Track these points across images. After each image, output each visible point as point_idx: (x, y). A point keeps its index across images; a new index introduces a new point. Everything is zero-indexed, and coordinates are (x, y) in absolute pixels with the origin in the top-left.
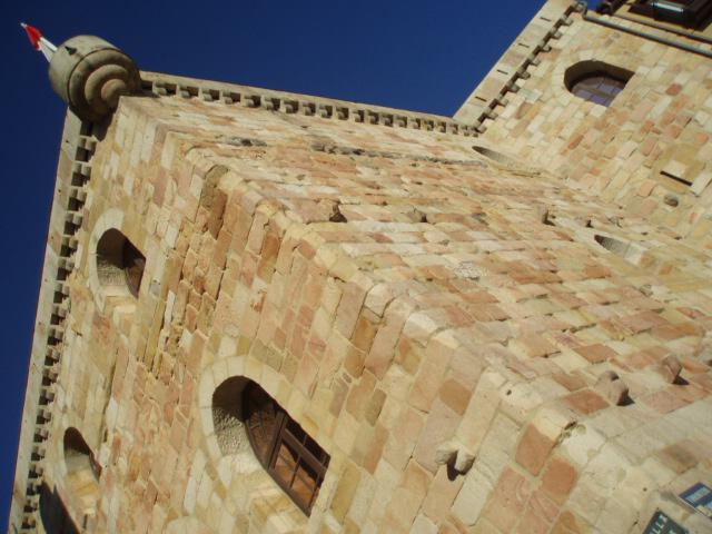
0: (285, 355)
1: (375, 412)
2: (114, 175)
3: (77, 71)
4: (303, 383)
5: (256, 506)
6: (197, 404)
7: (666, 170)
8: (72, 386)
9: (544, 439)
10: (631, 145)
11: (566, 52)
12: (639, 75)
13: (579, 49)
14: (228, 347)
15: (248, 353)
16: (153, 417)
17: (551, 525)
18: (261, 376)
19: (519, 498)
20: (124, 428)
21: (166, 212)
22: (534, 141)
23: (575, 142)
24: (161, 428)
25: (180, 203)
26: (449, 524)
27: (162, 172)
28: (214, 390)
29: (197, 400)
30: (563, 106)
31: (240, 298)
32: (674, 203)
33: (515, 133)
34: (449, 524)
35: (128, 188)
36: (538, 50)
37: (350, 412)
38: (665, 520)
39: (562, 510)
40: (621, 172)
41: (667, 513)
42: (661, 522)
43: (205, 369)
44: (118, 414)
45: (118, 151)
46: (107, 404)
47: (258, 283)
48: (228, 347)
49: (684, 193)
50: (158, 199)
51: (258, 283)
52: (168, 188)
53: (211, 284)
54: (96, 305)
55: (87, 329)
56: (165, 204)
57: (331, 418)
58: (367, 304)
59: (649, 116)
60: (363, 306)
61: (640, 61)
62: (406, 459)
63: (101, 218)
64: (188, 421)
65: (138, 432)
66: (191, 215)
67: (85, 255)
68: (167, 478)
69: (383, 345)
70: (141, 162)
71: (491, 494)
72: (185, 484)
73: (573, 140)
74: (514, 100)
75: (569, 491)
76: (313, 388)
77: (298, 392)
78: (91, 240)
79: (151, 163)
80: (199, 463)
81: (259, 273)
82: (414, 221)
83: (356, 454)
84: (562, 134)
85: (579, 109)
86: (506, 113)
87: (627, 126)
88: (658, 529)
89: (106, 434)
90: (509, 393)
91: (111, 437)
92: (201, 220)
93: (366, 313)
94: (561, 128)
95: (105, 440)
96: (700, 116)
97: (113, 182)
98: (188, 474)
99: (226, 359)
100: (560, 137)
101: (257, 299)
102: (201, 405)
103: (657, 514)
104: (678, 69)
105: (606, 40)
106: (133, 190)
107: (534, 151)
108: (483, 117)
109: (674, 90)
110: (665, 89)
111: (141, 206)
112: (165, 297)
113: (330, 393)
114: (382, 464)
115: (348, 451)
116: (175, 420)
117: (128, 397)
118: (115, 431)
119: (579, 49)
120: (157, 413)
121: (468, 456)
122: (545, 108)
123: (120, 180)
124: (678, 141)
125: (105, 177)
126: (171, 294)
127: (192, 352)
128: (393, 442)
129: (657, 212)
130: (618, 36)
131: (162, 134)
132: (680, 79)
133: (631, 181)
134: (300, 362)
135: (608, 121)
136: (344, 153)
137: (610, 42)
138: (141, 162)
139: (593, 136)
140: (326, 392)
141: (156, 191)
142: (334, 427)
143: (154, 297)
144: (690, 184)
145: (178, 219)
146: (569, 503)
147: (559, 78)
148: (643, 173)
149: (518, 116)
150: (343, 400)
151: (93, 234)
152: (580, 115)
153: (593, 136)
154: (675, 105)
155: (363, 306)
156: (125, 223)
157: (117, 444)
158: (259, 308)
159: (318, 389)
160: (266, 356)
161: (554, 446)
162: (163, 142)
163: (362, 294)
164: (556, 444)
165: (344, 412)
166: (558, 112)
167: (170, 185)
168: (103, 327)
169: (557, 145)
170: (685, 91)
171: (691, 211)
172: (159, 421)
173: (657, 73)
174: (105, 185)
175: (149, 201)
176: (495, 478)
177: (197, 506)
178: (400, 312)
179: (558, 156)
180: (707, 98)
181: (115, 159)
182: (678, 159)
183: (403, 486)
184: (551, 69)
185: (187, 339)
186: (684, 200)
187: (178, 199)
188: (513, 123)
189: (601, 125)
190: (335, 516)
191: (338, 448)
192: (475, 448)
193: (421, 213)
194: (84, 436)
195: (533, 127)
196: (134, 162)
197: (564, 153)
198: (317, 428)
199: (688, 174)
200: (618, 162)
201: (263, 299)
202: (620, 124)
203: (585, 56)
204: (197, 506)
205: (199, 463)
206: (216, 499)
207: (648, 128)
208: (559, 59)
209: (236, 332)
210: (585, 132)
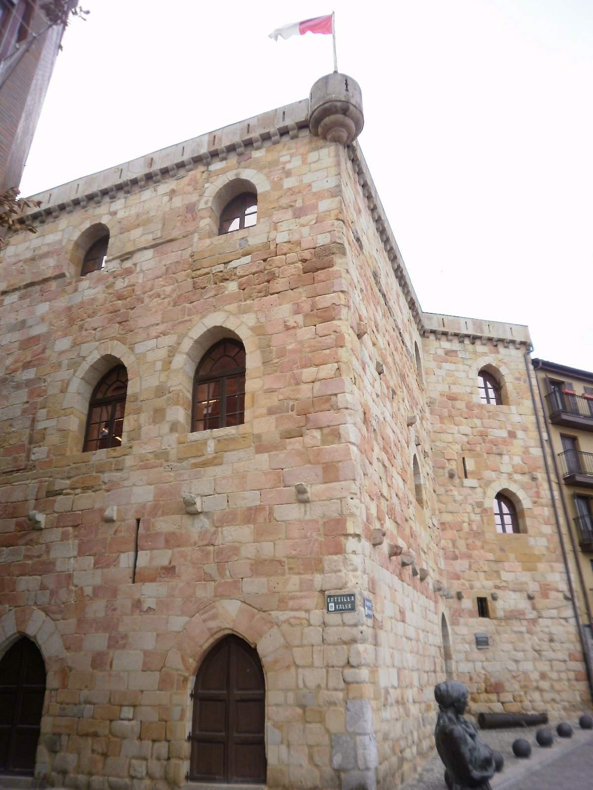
0: (275, 361)
1: (288, 435)
2: (288, 166)
4: (269, 383)
5: (178, 394)
6: (201, 318)
7: (466, 459)
8: (133, 211)
9: (345, 528)
10: (468, 430)
11: (500, 357)
12: (510, 409)
13: (505, 363)
14: (250, 319)
15: (257, 335)
16: (168, 289)
17: (309, 556)
18: (251, 352)
19: (309, 534)
20: (142, 271)
21: (292, 224)
22: (438, 372)
23: (452, 398)
24: (166, 300)
25: (306, 231)
26: (267, 508)
27: (315, 207)
28: (219, 325)
29: (203, 317)
30: (467, 377)
31: (283, 311)
32: (451, 476)
33: (436, 358)
34: (267, 508)
35: (288, 183)
36: (490, 339)
37: (277, 421)
38: (353, 599)
39: (321, 556)
40: (451, 435)
41: (356, 598)
42: (350, 598)
43: (226, 311)
44: (146, 260)
45: (304, 162)
46: (145, 248)
47: (300, 318)
48: (250, 319)
49: (459, 478)
50: (299, 213)
51: (300, 318)
52: (309, 217)
53: (279, 284)
54: (199, 201)
55: (178, 202)
56: (297, 220)
57: (264, 411)
58: (339, 395)
59: (490, 430)
60: (336, 395)
61: (518, 404)
62: (279, 467)
63: (255, 171)
64: (187, 318)
65: (150, 283)
66: (304, 245)
67: (223, 171)
68: (142, 323)
69: (325, 417)
70: (310, 185)
71: (300, 520)
72: (149, 338)
73: (451, 395)
74: (455, 345)
75: (332, 554)
76: (273, 391)
77: (261, 382)
78: (235, 172)
79: (315, 194)
80: (170, 340)
81: (306, 316)
82: (377, 369)
83: (258, 437)
84: (452, 387)
85: (472, 387)
86: (446, 345)
87: (478, 422)
88: (347, 599)
89: (127, 259)
90: (352, 499)
91: (128, 264)
92: (307, 255)
93: (333, 398)
94: (455, 384)
95: (122, 261)
96: (506, 458)
97: (283, 168)
98: (157, 337)
99: (243, 322)
100: (449, 387)
101: (291, 323)
102: (203, 321)
103: (353, 595)
104: (525, 430)
105: (519, 376)
106: (289, 189)
107: (433, 376)
108: (433, 332)
109: (512, 435)
110: (510, 429)
111: (284, 201)
112: (245, 255)
113: (276, 403)
114: (265, 456)
115: (256, 431)
116: (180, 307)
117: (163, 263)
118: (135, 265)
119: (505, 363)
120: (174, 291)
121: (308, 498)
122: (461, 367)
123: (288, 174)
124: (485, 455)
125: (283, 159)
126: (248, 258)
127: (229, 295)
128: (282, 455)
129: (441, 470)
130: (525, 382)
131: (337, 192)
132: (520, 434)
133: (449, 444)
134: (278, 374)
135: (475, 408)
136: (380, 290)
137: (518, 379)
138: (310, 185)
139: (461, 405)
140: (274, 400)
141: (301, 209)
142: (262, 416)
143: (238, 246)
144: (466, 477)
145: (296, 237)
146: (325, 557)
147: (482, 363)
148: (457, 447)
149: (447, 353)
150: (280, 413)
151: (240, 170)
152: (469, 390)
153: (461, 405)
154: (504, 441)
155: (336, 395)
156: (266, 194)
157: (129, 272)
158: (288, 328)
159: (273, 394)
160: (265, 348)
161: (344, 535)
162: (332, 196)
163: (342, 391)
164: (347, 535)
165: (274, 417)
166: (463, 375)
167: (310, 218)
168: (189, 215)
169: (443, 388)
170: (515, 441)
171: (452, 488)
172: (169, 296)
173: (516, 419)
174: (276, 163)
175: (291, 206)
176: (308, 517)
177: (144, 355)
178: (348, 418)
179: (439, 393)
180: (518, 455)
181: (296, 162)
182: (476, 463)
183: (265, 474)
184: (485, 354)
185: (232, 287)
186: (457, 481)
187: (307, 229)
188: (441, 352)
189: (470, 407)
190: (216, 446)
191: (252, 425)
192: (314, 499)
193: (383, 370)
194: (110, 240)
195: (447, 366)
196: (307, 179)
197: (442, 395)
198: (253, 406)
199: (472, 473)
200: (455, 429)
201: (294, 327)
202: (477, 417)
203: (503, 370)
204: (144, 355)
205: (170, 340)
206: (159, 366)
207: (483, 435)
208: (493, 355)
209: (263, 320)
210: (461, 400)
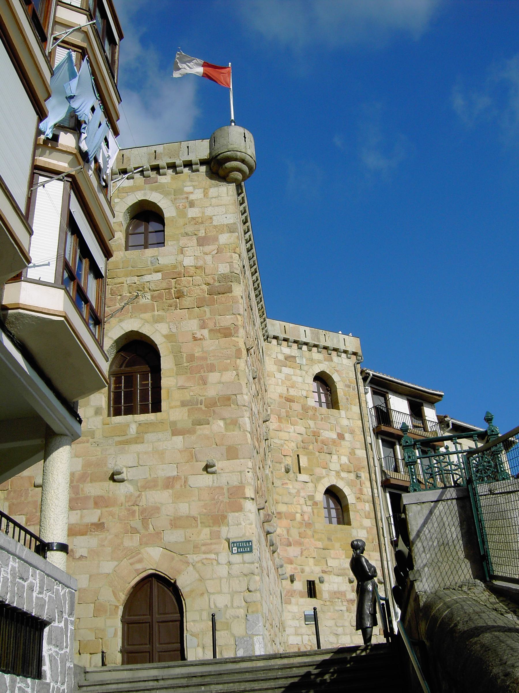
0: (185, 365)
3: (239, 153)
7: (300, 456)
9: (244, 493)
10: (302, 430)
11: (333, 364)
12: (340, 413)
13: (337, 371)
17: (217, 513)
18: (165, 356)
19: (216, 497)
21: (199, 251)
22: (278, 375)
23: (290, 400)
25: (209, 258)
26: (183, 477)
27: (216, 239)
30: (304, 381)
32: (287, 471)
33: (277, 362)
34: (183, 477)
35: (192, 213)
36: (325, 348)
38: (250, 544)
39: (226, 514)
40: (288, 433)
45: (206, 194)
47: (205, 332)
49: (294, 473)
50: (202, 242)
51: (205, 332)
53: (187, 302)
57: (179, 403)
59: (322, 431)
61: (347, 409)
62: (192, 447)
69: (226, 412)
71: (209, 487)
73: (289, 397)
74: (294, 351)
75: (234, 512)
79: (215, 227)
81: (211, 331)
84: (290, 389)
85: (307, 391)
86: (285, 350)
87: (311, 423)
88: (246, 544)
90: (248, 472)
94: (292, 387)
96: (335, 457)
97: (187, 198)
99: (157, 330)
100: (288, 389)
101: (198, 336)
104: (352, 432)
105: (349, 384)
107: (273, 379)
108: (275, 338)
109: (341, 436)
110: (339, 432)
113: (188, 398)
115: (172, 419)
119: (337, 371)
122: (298, 371)
123: (192, 204)
124: (317, 453)
125: (187, 189)
128: (193, 438)
129: (278, 465)
130: (354, 390)
132: (347, 436)
133: (286, 442)
134: (189, 375)
135: (309, 411)
137: (349, 387)
139: (297, 407)
140: (187, 396)
144: (300, 473)
145: (200, 263)
146: (229, 514)
147: (317, 370)
148: (293, 445)
149: (287, 358)
150: (191, 405)
152: (304, 393)
153: (297, 407)
154: (334, 441)
158: (195, 339)
160: (177, 354)
165: (186, 408)
166: (300, 379)
167: (211, 248)
169: (281, 390)
170: (343, 443)
171: (288, 482)
173: (345, 422)
176: (215, 485)
179: (278, 395)
180: (345, 455)
182: (308, 459)
183: (181, 452)
184: (320, 362)
186: (291, 474)
188: (281, 357)
189: (305, 409)
191: (168, 414)
192: (220, 472)
195: (285, 370)
196: (209, 212)
197: (281, 396)
198: (168, 399)
199: (305, 468)
200: (291, 429)
201: (200, 339)
202: (311, 419)
203: (336, 377)
207: (316, 435)
208: (327, 363)
209: (174, 330)
210: (297, 402)
